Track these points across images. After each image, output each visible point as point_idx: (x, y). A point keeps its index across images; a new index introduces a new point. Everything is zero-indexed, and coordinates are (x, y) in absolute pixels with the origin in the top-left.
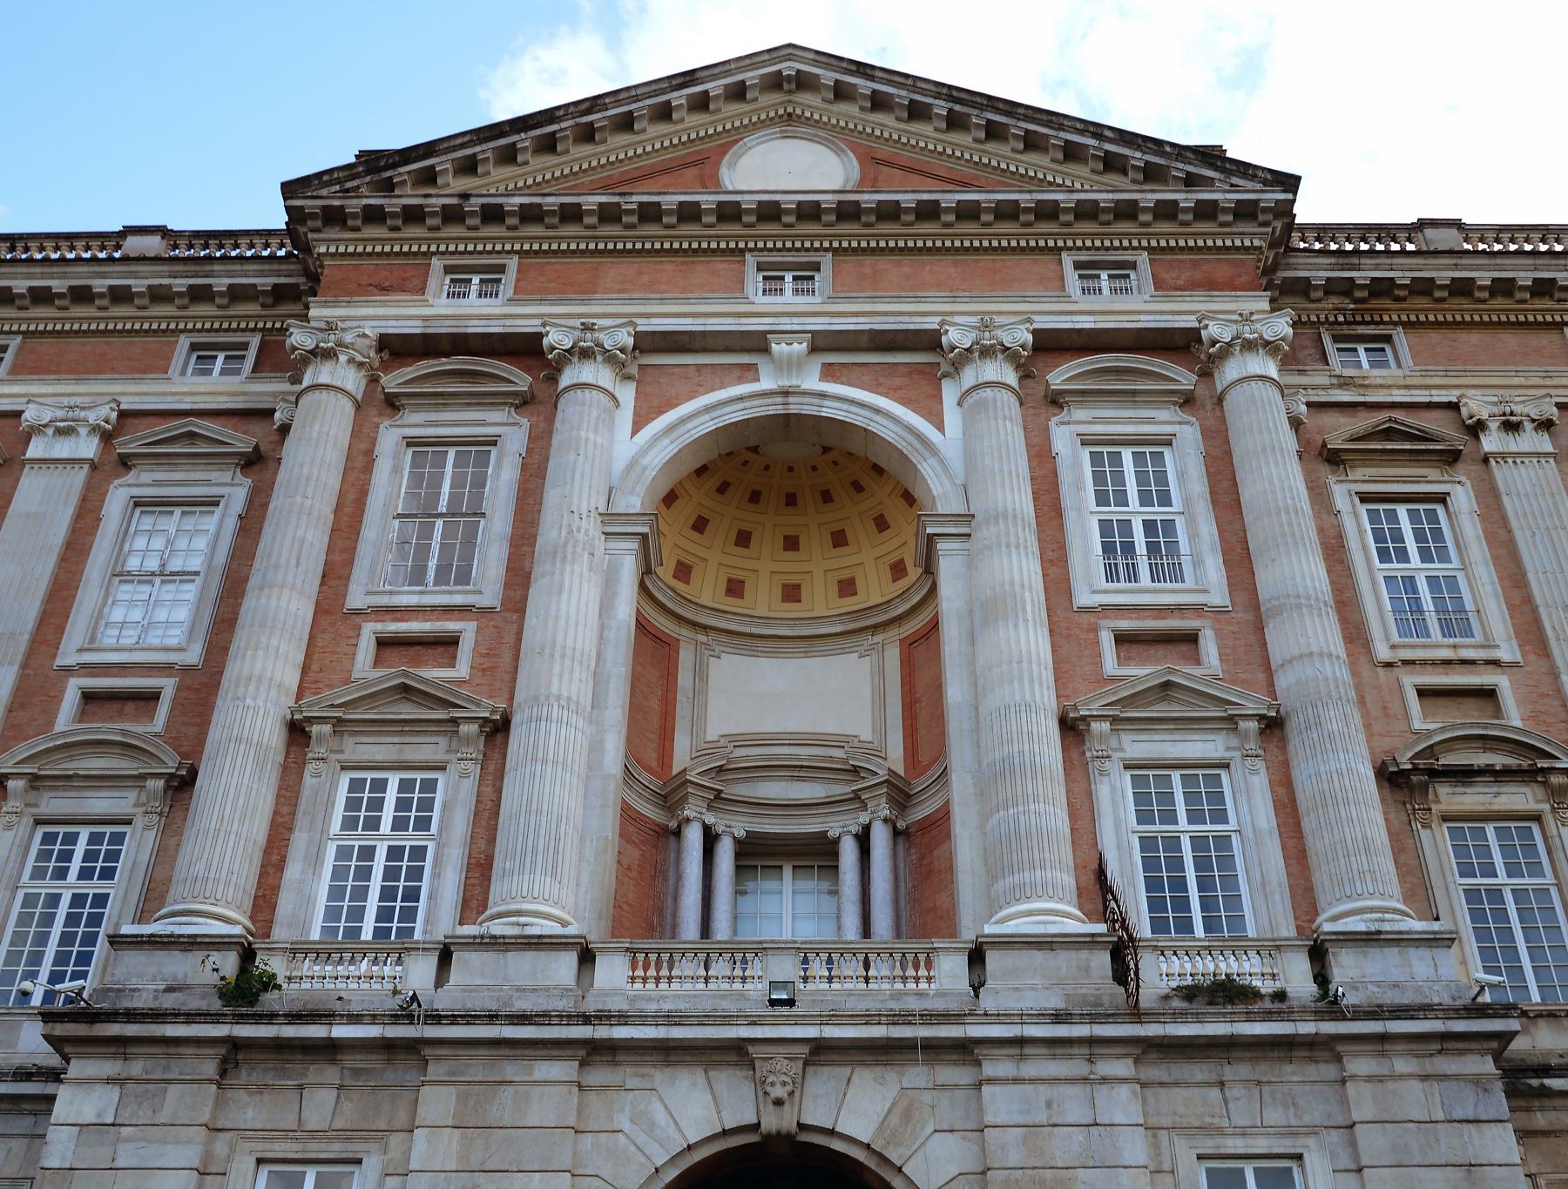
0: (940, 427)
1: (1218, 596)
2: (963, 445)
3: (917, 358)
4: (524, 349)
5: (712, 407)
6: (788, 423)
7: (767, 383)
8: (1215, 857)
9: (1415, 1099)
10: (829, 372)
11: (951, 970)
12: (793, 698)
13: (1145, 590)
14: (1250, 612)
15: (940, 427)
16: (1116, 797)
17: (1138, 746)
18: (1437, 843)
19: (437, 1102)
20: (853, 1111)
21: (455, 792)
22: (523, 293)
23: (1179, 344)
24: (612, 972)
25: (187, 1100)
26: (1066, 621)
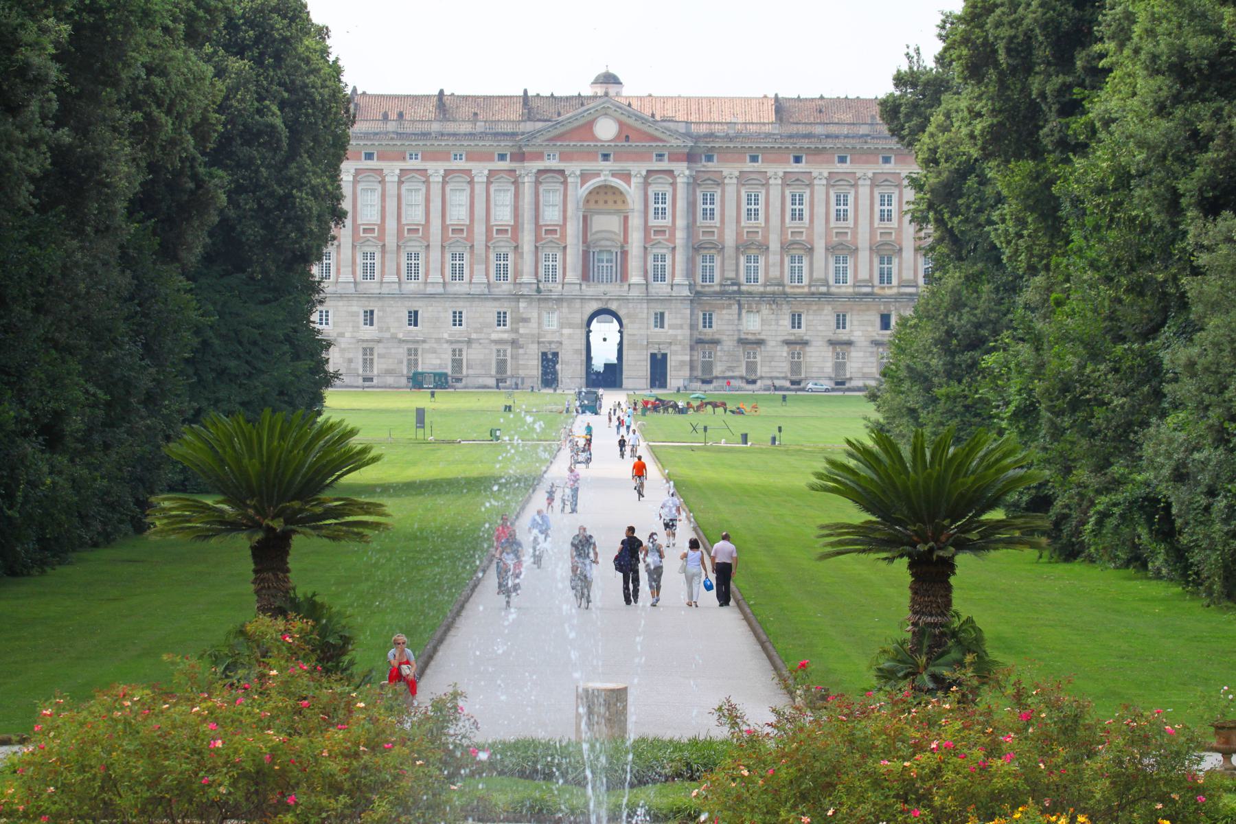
0: (629, 185)
1: (670, 224)
2: (632, 191)
3: (626, 177)
4: (562, 172)
5: (592, 183)
6: (606, 186)
7: (602, 178)
8: (663, 267)
9: (679, 305)
10: (613, 175)
11: (626, 287)
12: (607, 223)
13: (660, 222)
14: (673, 228)
15: (629, 185)
16: (650, 258)
17: (655, 251)
18: (699, 259)
19: (565, 304)
20: (613, 306)
21: (559, 256)
22: (561, 160)
23: (670, 172)
24: (584, 287)
25: (535, 304)
26: (646, 228)
